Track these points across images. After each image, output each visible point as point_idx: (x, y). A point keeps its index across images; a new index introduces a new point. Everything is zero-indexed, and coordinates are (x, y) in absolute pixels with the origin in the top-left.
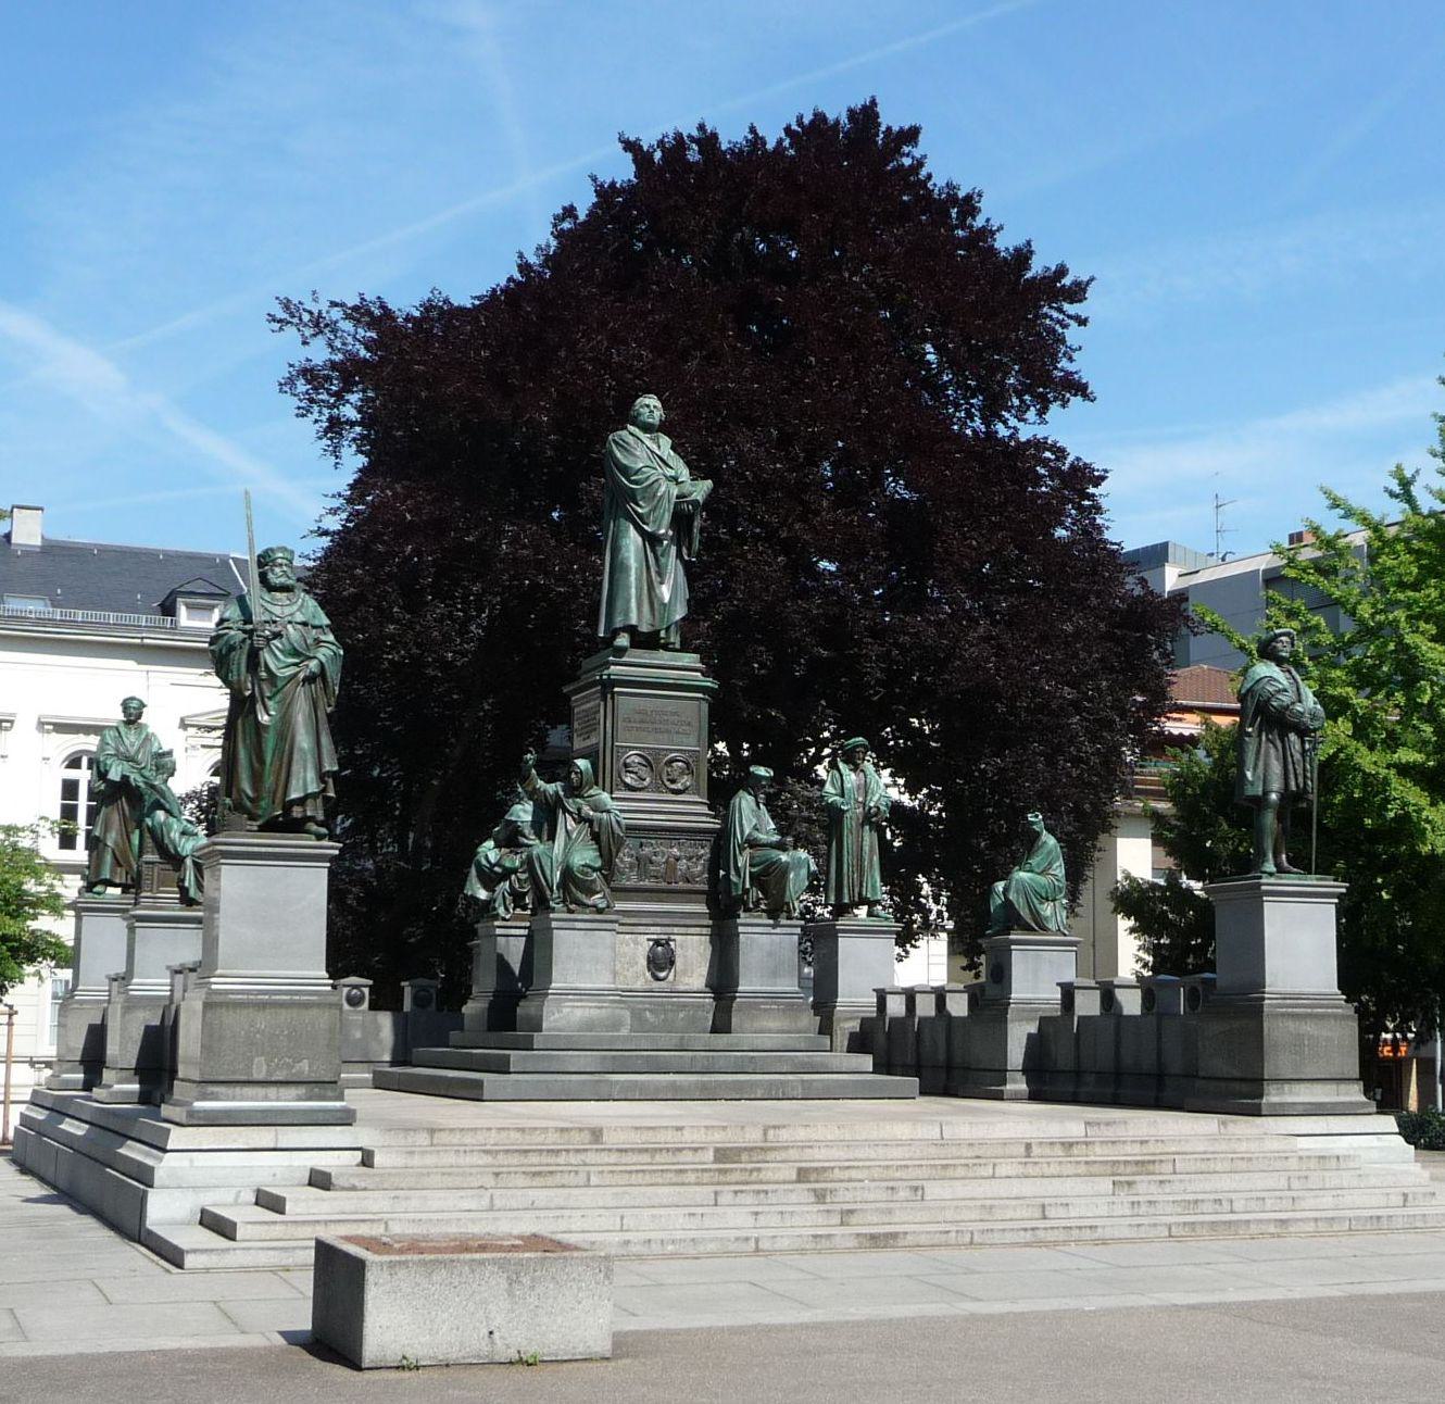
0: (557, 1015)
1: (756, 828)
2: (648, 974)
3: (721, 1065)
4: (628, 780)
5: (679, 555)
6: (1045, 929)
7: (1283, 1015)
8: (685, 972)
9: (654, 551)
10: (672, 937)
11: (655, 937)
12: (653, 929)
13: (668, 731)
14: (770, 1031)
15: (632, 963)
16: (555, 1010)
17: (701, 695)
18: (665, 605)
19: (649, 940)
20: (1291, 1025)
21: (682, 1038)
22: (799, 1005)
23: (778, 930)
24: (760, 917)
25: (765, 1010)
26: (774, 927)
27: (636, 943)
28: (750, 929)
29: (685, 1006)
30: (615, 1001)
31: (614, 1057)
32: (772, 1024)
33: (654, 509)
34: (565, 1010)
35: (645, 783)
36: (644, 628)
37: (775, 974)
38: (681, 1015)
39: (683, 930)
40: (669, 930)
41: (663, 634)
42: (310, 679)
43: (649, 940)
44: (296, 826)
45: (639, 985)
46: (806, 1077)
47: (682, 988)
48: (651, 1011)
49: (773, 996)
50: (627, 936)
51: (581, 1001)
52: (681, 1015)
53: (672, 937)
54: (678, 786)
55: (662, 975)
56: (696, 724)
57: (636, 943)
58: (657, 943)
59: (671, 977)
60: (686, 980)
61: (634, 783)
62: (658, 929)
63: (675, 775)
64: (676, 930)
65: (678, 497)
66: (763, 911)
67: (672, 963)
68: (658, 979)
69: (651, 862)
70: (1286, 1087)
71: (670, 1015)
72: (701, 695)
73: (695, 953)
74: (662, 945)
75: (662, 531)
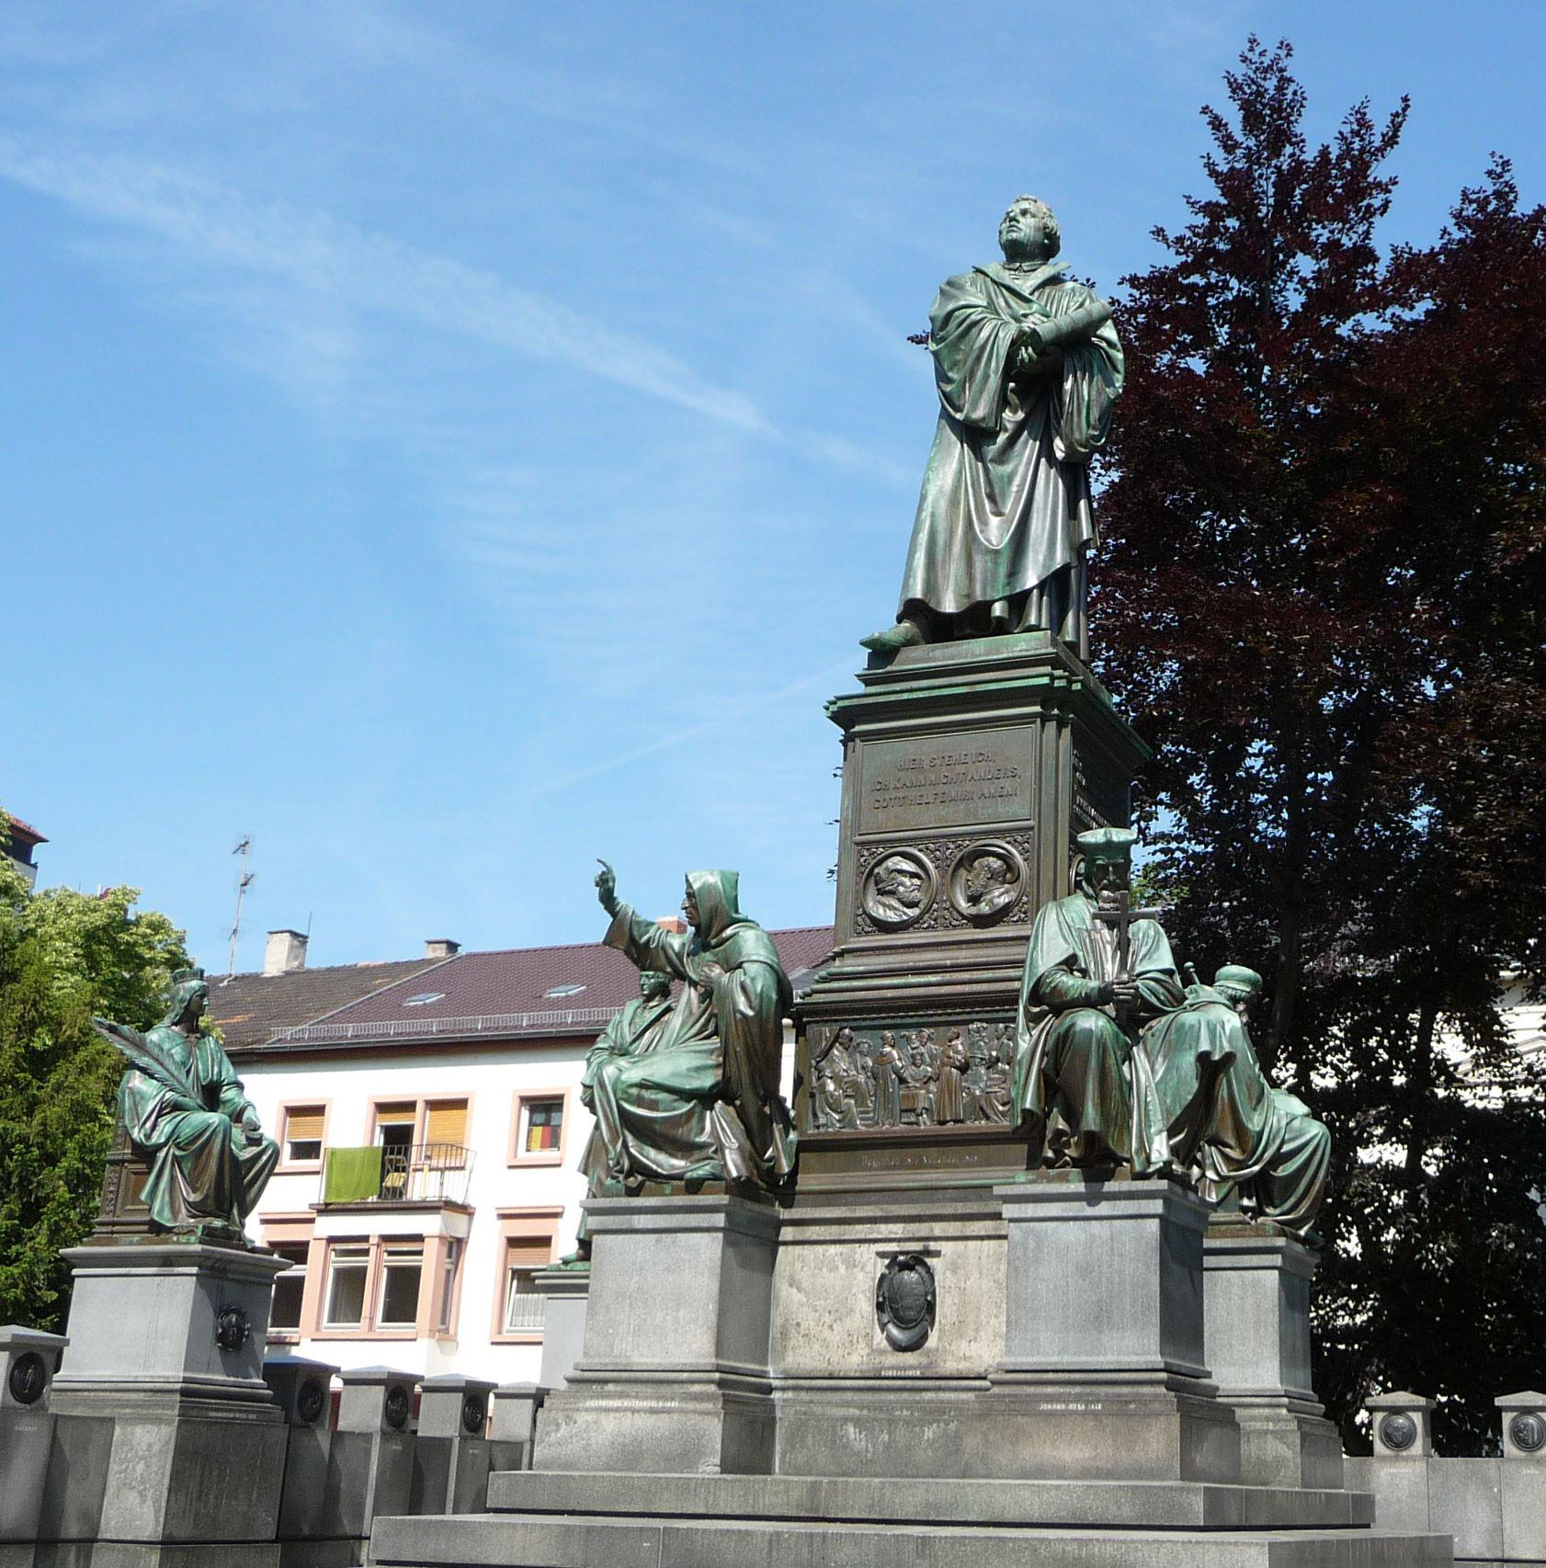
4: (880, 913)
5: (1047, 451)
8: (959, 1329)
9: (978, 454)
11: (893, 1247)
12: (885, 1230)
13: (967, 798)
15: (842, 1311)
17: (1038, 709)
18: (997, 552)
19: (882, 1255)
21: (814, 1487)
23: (1104, 1208)
24: (1064, 1178)
25: (1052, 1414)
26: (1093, 1198)
27: (851, 1264)
28: (1030, 1210)
29: (938, 1412)
32: (1071, 1452)
33: (972, 373)
36: (949, 604)
37: (1099, 1319)
40: (922, 1229)
41: (998, 610)
43: (882, 1255)
45: (856, 1360)
47: (950, 1366)
48: (857, 1422)
50: (833, 1249)
52: (929, 1433)
53: (933, 1246)
54: (984, 908)
56: (1030, 773)
57: (851, 1264)
58: (899, 1263)
59: (932, 1341)
60: (963, 1347)
62: (897, 1229)
63: (977, 887)
64: (938, 1228)
65: (1013, 343)
68: (899, 1348)
71: (901, 1433)
72: (1038, 709)
73: (986, 1284)
75: (979, 414)
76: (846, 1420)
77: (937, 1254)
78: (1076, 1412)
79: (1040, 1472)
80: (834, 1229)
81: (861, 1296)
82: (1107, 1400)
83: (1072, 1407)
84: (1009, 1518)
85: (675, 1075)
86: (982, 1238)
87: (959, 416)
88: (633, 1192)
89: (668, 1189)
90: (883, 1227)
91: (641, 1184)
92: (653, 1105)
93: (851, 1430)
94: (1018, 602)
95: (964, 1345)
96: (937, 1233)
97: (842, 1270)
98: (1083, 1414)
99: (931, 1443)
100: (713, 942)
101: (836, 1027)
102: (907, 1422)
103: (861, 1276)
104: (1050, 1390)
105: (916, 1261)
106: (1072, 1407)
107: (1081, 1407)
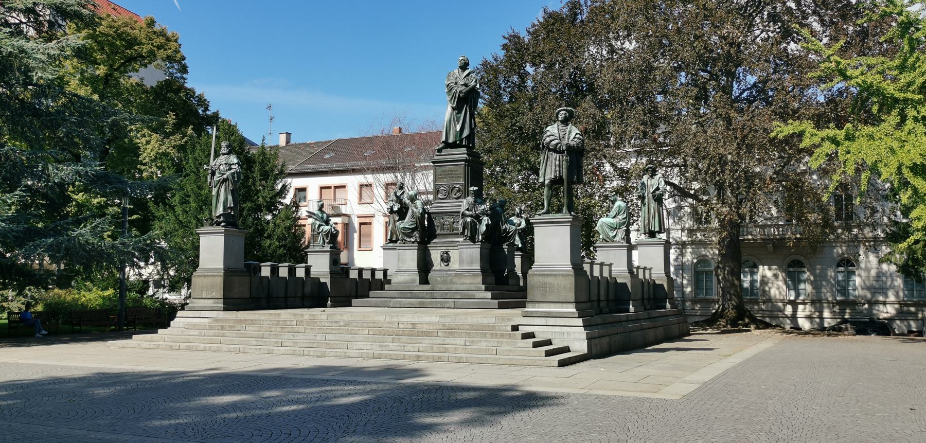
1: (468, 210)
3: (436, 295)
6: (613, 241)
7: (536, 275)
20: (540, 278)
42: (225, 180)
44: (218, 224)
49: (469, 271)
70: (537, 305)
105: (447, 253)
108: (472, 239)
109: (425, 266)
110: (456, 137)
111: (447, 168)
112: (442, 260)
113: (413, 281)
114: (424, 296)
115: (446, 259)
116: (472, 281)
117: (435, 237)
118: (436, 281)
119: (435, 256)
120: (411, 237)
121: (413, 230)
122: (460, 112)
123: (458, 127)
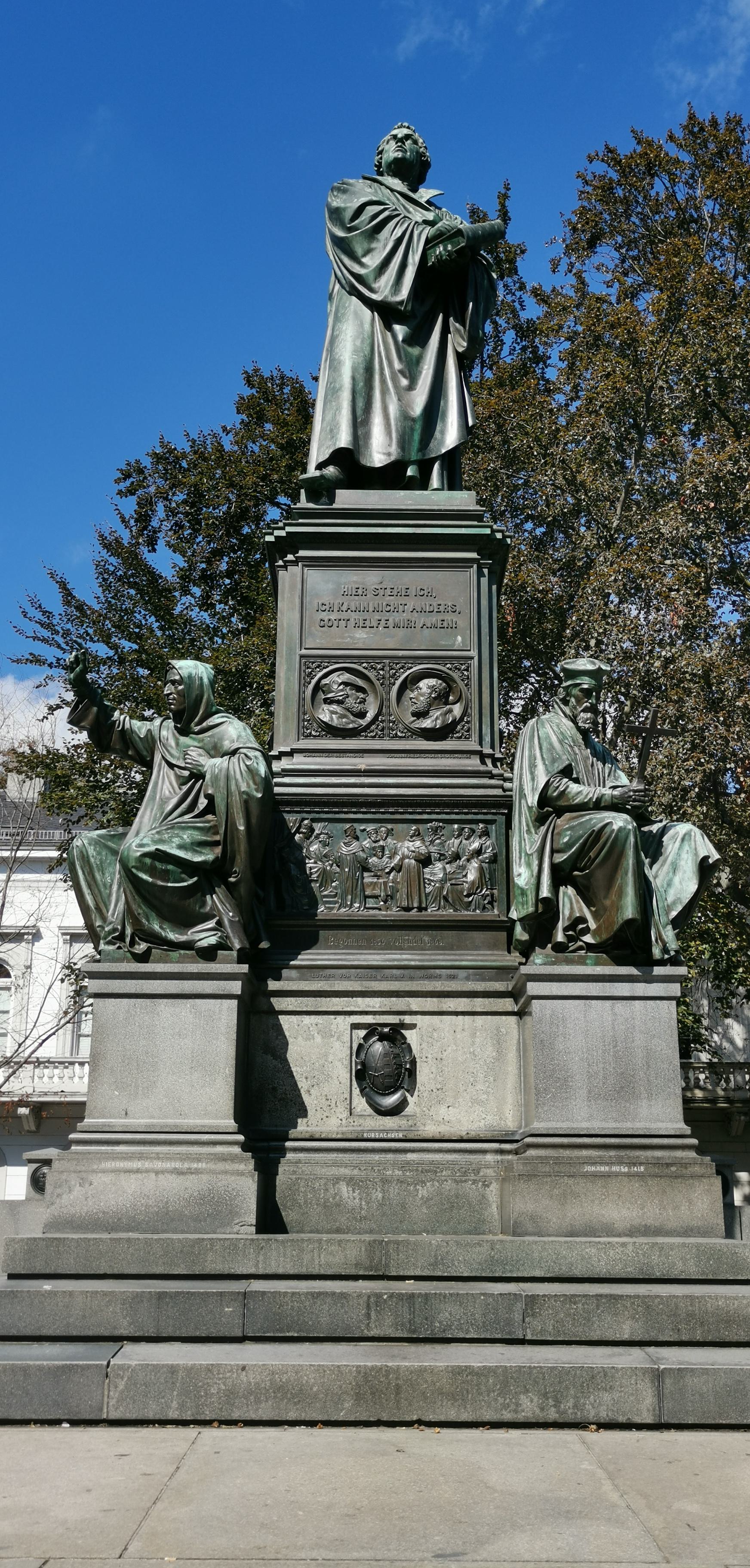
0: (78, 1191)
1: (567, 772)
2: (361, 1104)
3: (447, 1316)
10: (408, 1019)
11: (369, 1019)
12: (361, 1003)
14: (610, 1231)
16: (74, 1180)
17: (474, 555)
18: (414, 420)
19: (355, 1026)
22: (684, 1165)
24: (582, 962)
25: (595, 1175)
30: (223, 1158)
31: (161, 1296)
34: (99, 1180)
35: (364, 722)
37: (624, 1088)
38: (422, 1192)
39: (430, 1004)
46: (672, 1358)
47: (430, 1129)
48: (351, 1181)
49: (625, 1144)
50: (307, 1020)
51: (141, 1157)
52: (422, 1192)
53: (408, 1019)
55: (392, 1100)
57: (327, 1034)
60: (443, 1111)
61: (336, 722)
62: (375, 1003)
64: (415, 1004)
66: (589, 947)
67: (412, 1073)
69: (365, 868)
72: (474, 555)
74: (382, 1038)
76: (337, 1180)
77: (413, 1026)
78: (617, 1175)
79: (590, 1231)
80: (311, 1000)
81: (339, 1064)
82: (657, 1163)
83: (615, 1168)
84: (577, 1272)
85: (675, 826)
86: (456, 1013)
87: (374, 296)
88: (143, 958)
89: (175, 955)
90: (360, 1000)
91: (148, 952)
92: (165, 875)
93: (344, 1188)
94: (425, 467)
95: (443, 1111)
96: (415, 1008)
97: (318, 1039)
98: (629, 1175)
99: (426, 1201)
100: (197, 729)
101: (298, 817)
102: (400, 1181)
103: (337, 1045)
104: (585, 1153)
105: (394, 1035)
106: (615, 1168)
107: (626, 1170)
108: (629, 946)
109: (265, 1105)
110: (403, 443)
111: (372, 578)
112: (362, 1075)
113: (214, 1209)
114: (353, 1318)
115: (386, 1073)
116: (651, 1212)
117: (310, 941)
118: (332, 1207)
119: (319, 1051)
120: (187, 921)
121: (210, 876)
122: (418, 338)
123: (419, 400)
